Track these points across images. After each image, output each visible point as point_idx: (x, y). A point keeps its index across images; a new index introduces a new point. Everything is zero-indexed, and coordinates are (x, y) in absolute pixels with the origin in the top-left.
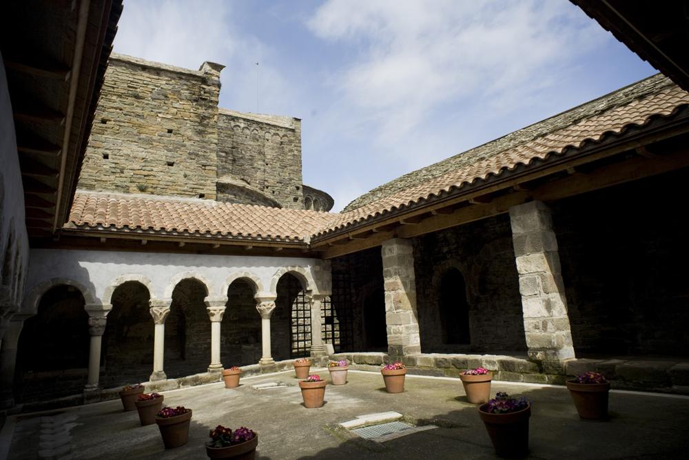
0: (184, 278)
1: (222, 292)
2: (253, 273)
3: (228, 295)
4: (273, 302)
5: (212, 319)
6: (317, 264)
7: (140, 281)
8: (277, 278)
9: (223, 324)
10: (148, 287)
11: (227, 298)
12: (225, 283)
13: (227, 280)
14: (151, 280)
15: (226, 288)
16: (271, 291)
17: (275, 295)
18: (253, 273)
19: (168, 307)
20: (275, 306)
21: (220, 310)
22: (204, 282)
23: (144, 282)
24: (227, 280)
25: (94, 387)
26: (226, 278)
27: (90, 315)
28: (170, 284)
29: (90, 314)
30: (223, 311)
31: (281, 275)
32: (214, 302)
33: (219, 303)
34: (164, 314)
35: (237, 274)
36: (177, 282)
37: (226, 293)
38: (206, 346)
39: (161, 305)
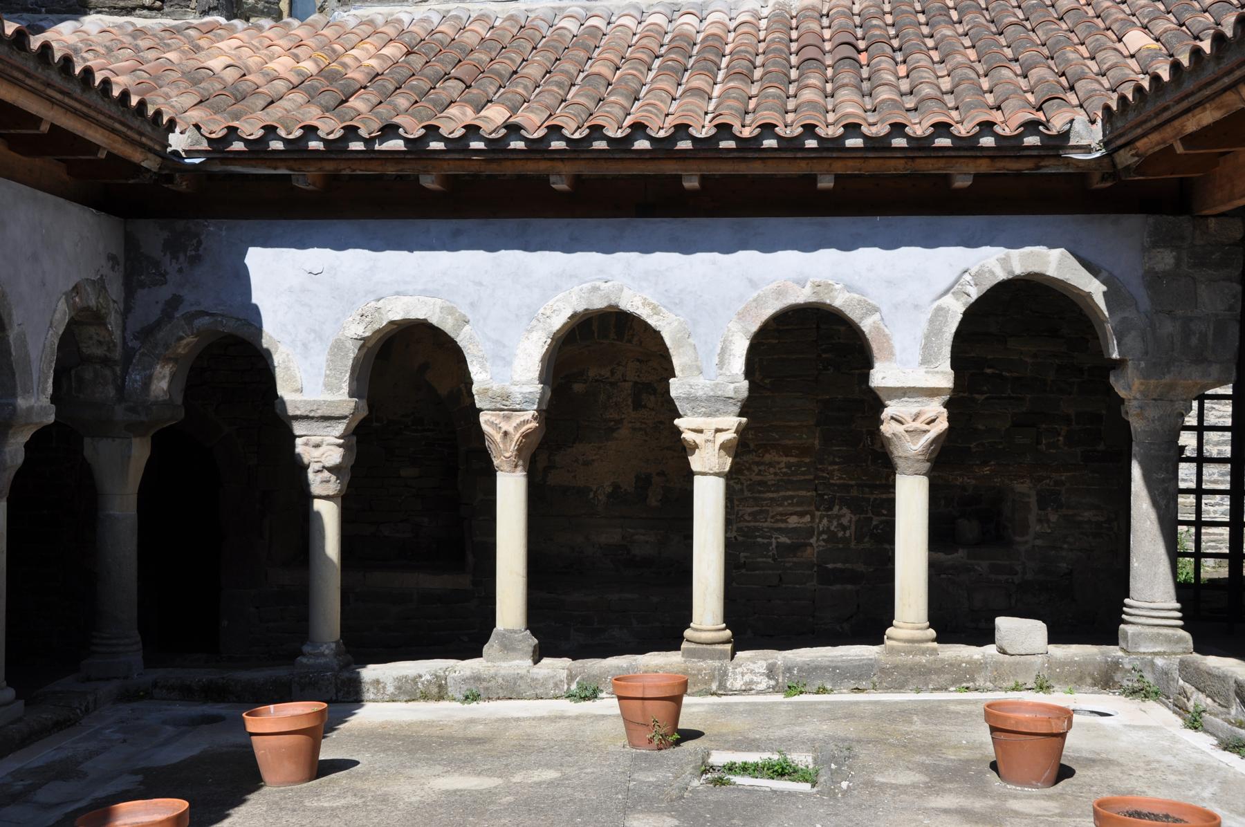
0: (580, 309)
1: (721, 364)
2: (849, 288)
3: (749, 374)
4: (936, 408)
5: (696, 462)
6: (1160, 240)
7: (434, 321)
8: (956, 309)
9: (734, 481)
10: (462, 340)
11: (746, 384)
12: (734, 326)
13: (741, 316)
14: (469, 317)
15: (741, 347)
16: (925, 361)
17: (943, 378)
18: (849, 288)
19: (529, 415)
20: (942, 425)
21: (718, 431)
22: (652, 321)
23: (447, 326)
24: (741, 316)
25: (323, 655)
26: (741, 307)
27: (297, 432)
28: (530, 331)
29: (298, 428)
30: (730, 435)
31: (975, 293)
32: (692, 399)
33: (714, 404)
34: (517, 436)
35: (780, 293)
36: (558, 321)
37: (738, 364)
38: (784, 539)
39: (506, 408)
